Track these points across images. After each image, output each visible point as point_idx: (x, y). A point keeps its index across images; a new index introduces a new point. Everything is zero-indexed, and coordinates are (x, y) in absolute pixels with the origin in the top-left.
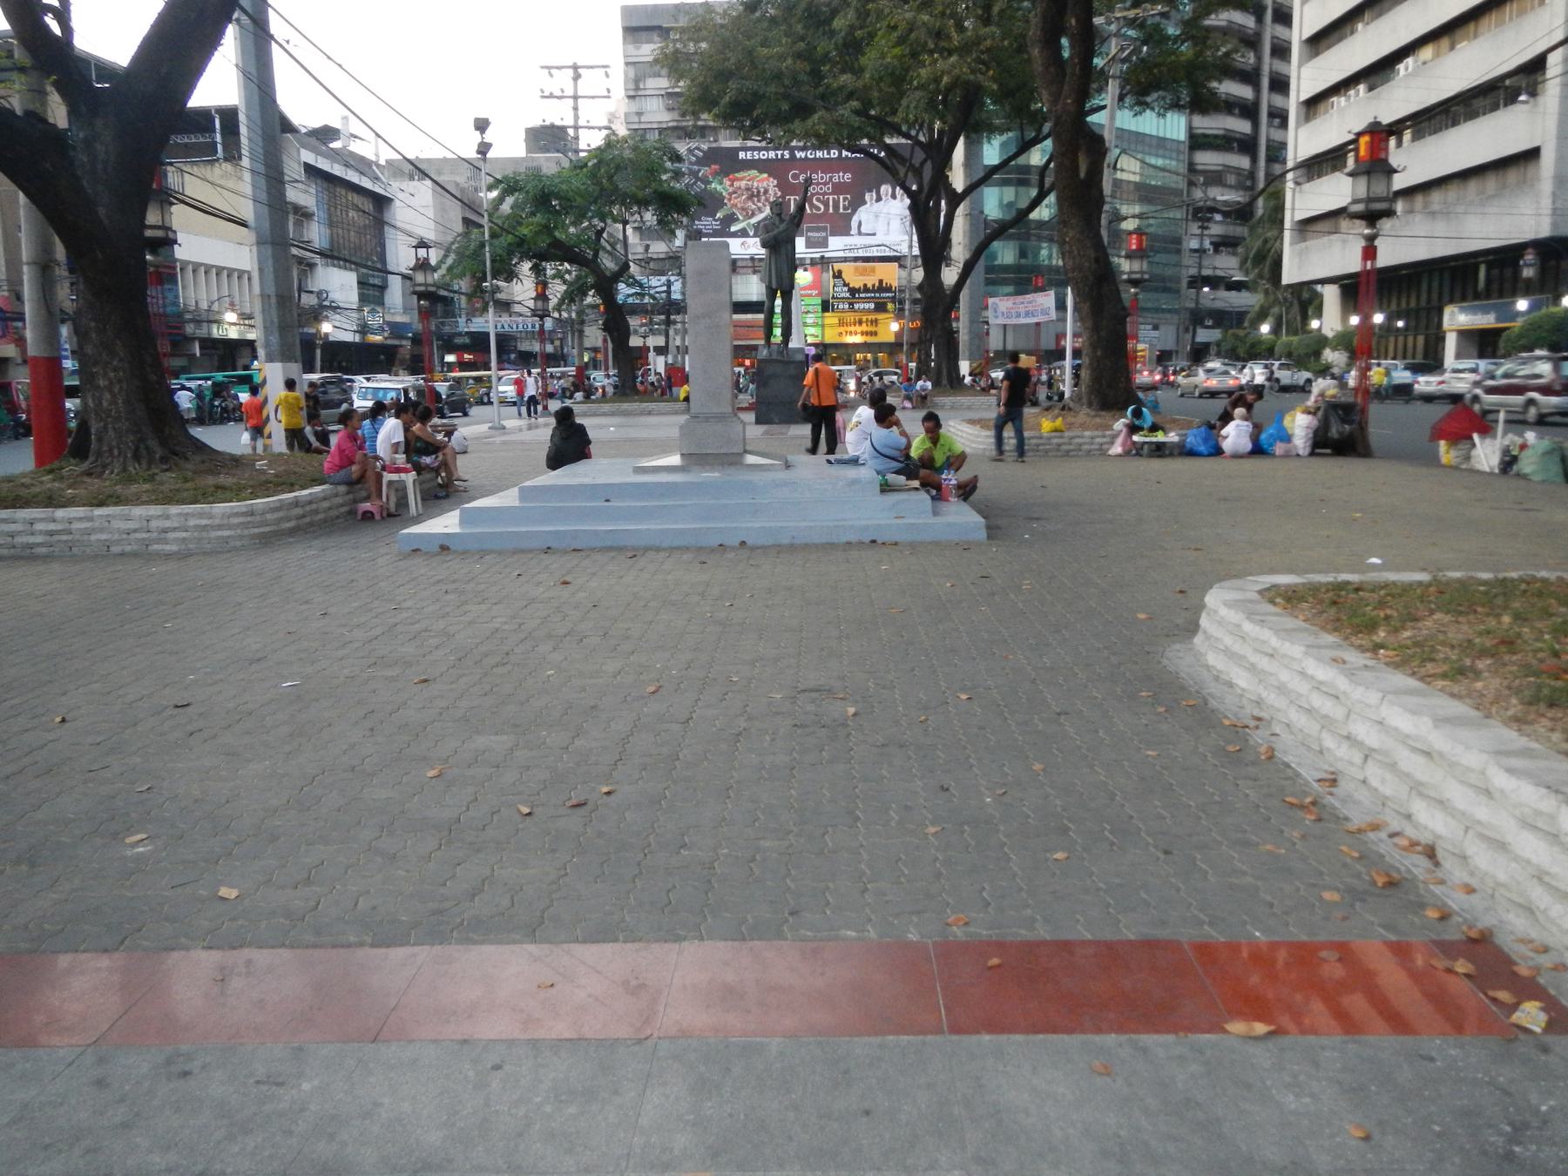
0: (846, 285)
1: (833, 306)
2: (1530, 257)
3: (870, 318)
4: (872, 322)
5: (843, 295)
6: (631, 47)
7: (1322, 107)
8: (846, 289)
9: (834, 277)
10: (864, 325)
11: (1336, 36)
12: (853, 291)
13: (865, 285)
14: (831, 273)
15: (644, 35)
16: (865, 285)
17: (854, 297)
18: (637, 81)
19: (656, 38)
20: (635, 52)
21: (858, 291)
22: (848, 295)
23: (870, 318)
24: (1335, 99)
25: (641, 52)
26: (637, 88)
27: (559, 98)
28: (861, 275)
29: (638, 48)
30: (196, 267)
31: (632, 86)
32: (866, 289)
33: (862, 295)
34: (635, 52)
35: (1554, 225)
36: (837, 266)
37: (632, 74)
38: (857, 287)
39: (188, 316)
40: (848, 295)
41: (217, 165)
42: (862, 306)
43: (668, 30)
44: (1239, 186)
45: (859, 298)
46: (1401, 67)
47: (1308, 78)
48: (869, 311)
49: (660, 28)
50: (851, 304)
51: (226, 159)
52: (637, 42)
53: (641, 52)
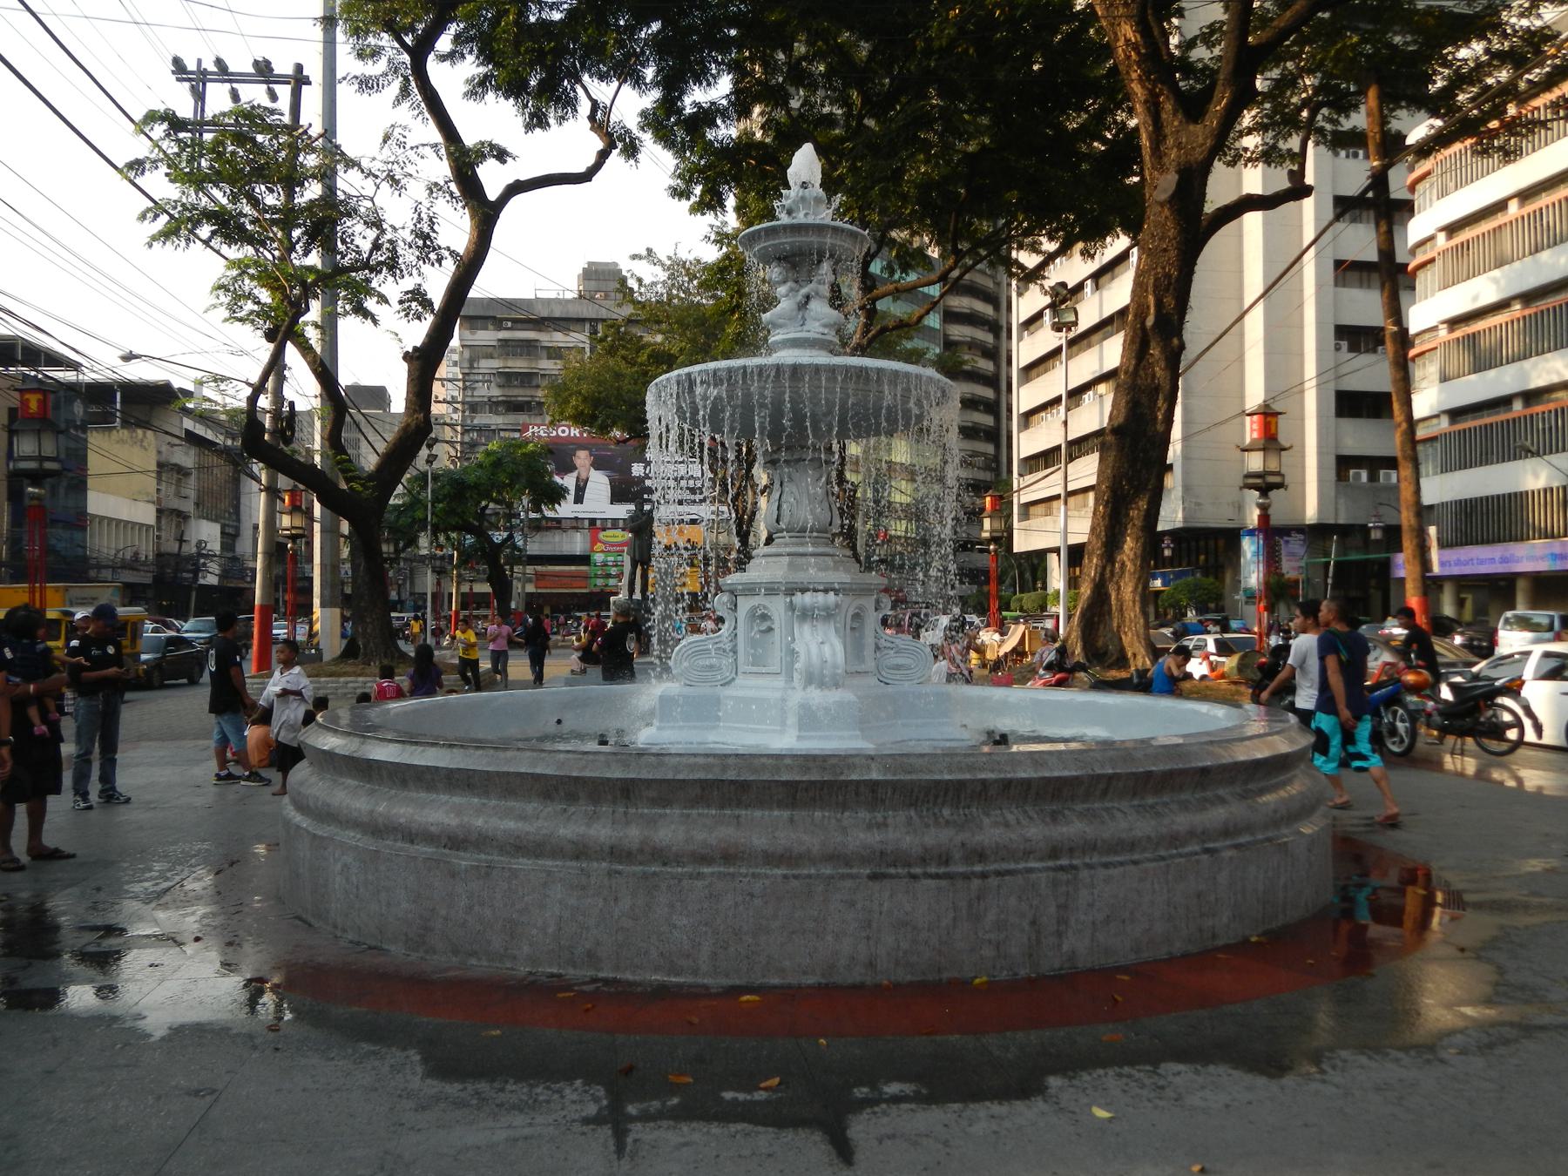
2: (1167, 541)
6: (467, 334)
7: (1036, 418)
11: (1041, 368)
15: (479, 322)
18: (472, 361)
19: (490, 327)
20: (471, 337)
24: (1043, 414)
25: (476, 337)
26: (471, 367)
27: (448, 403)
29: (473, 334)
30: (102, 518)
31: (466, 365)
34: (471, 337)
35: (1185, 519)
37: (467, 354)
39: (94, 562)
41: (115, 432)
43: (501, 320)
44: (987, 468)
46: (1086, 397)
47: (1026, 397)
49: (494, 318)
51: (123, 427)
52: (473, 328)
53: (476, 337)
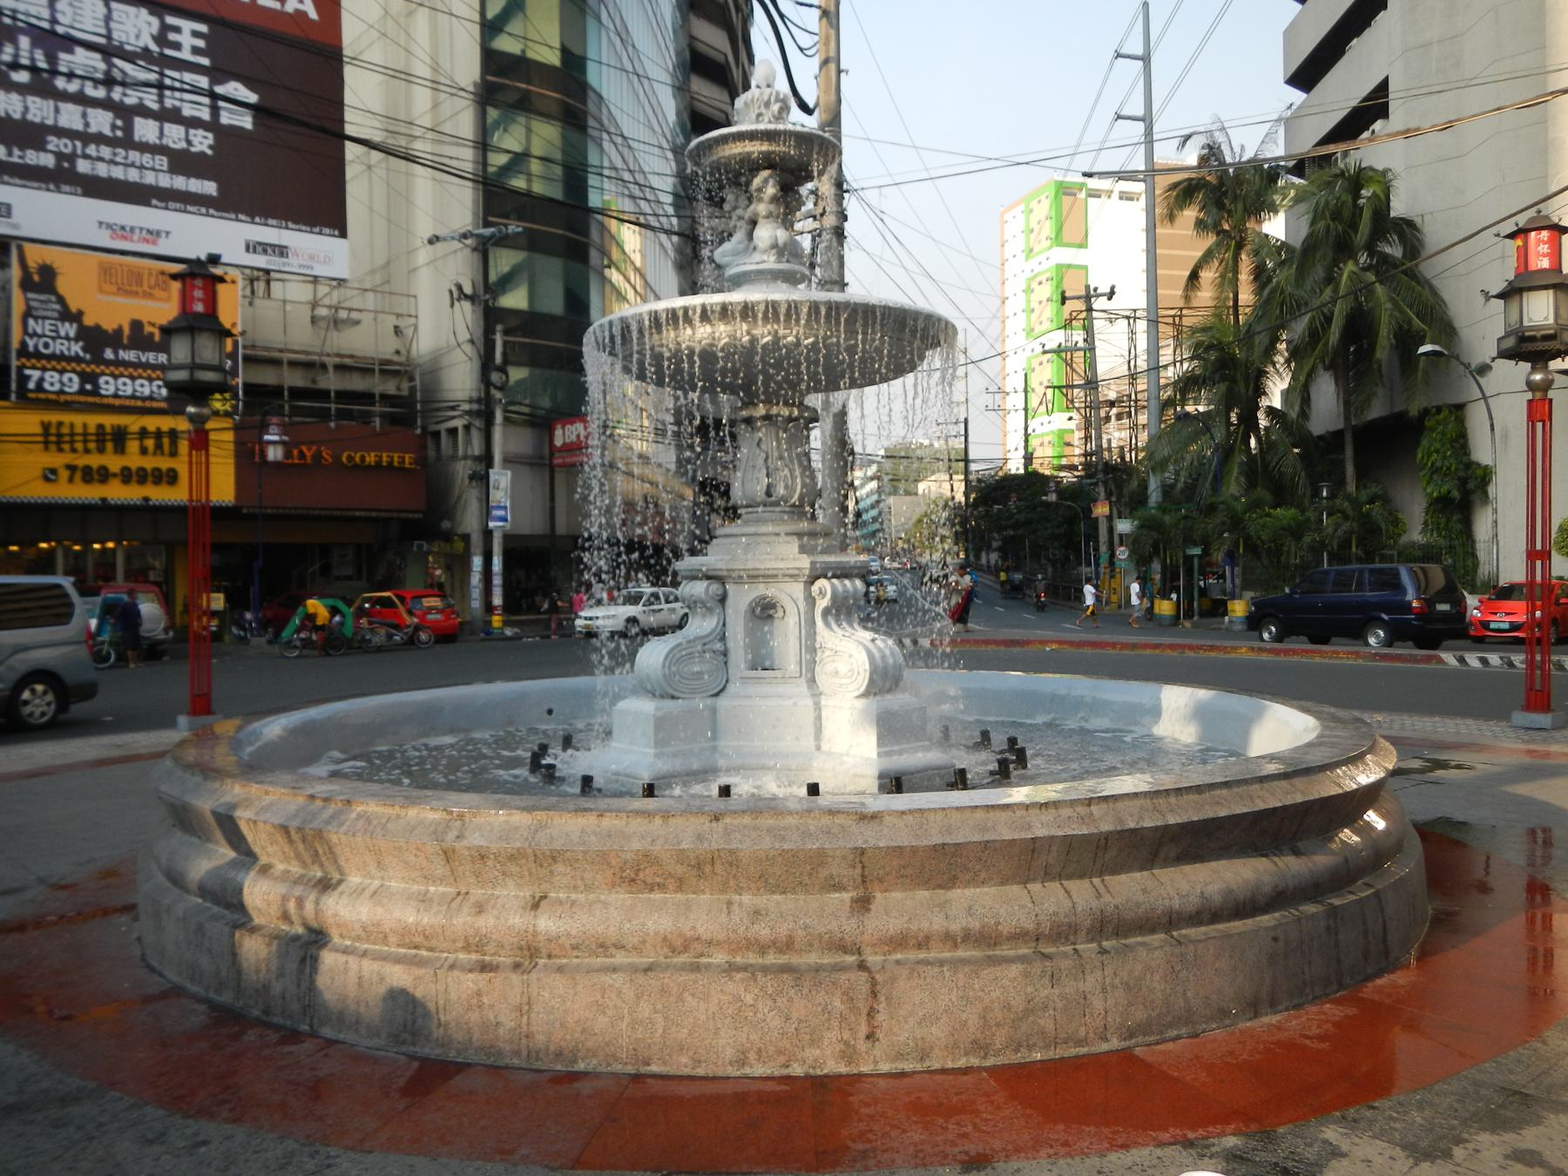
0: (67, 315)
1: (24, 379)
3: (152, 423)
4: (158, 435)
5: (58, 347)
8: (70, 329)
9: (27, 284)
10: (133, 446)
12: (95, 339)
13: (136, 325)
14: (15, 272)
16: (136, 325)
17: (99, 359)
21: (115, 339)
22: (76, 348)
23: (152, 423)
28: (122, 291)
32: (138, 337)
33: (129, 355)
36: (35, 255)
38: (109, 325)
40: (76, 348)
42: (127, 387)
45: (118, 363)
48: (143, 407)
50: (85, 377)
